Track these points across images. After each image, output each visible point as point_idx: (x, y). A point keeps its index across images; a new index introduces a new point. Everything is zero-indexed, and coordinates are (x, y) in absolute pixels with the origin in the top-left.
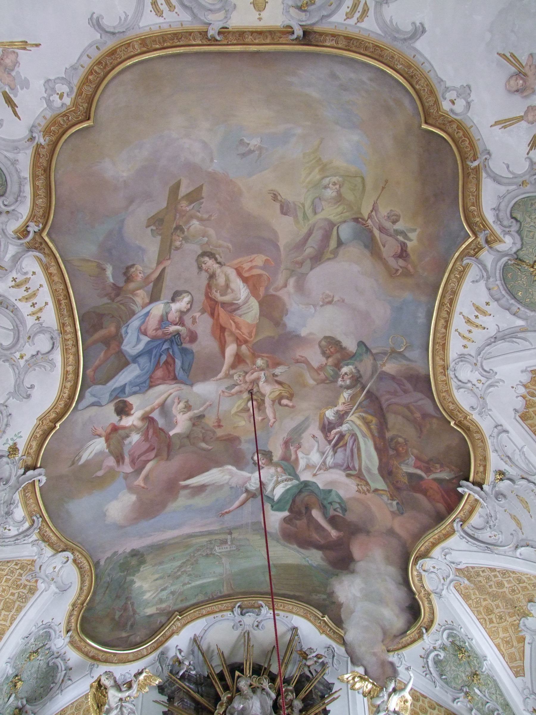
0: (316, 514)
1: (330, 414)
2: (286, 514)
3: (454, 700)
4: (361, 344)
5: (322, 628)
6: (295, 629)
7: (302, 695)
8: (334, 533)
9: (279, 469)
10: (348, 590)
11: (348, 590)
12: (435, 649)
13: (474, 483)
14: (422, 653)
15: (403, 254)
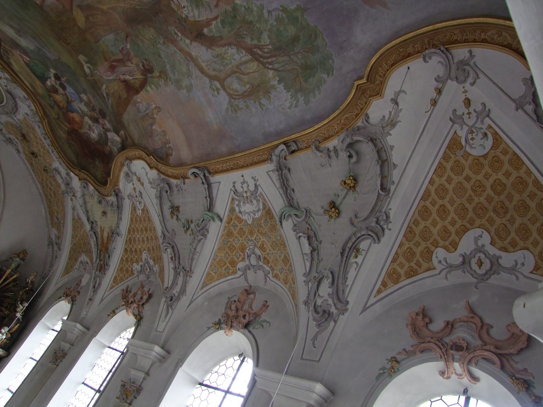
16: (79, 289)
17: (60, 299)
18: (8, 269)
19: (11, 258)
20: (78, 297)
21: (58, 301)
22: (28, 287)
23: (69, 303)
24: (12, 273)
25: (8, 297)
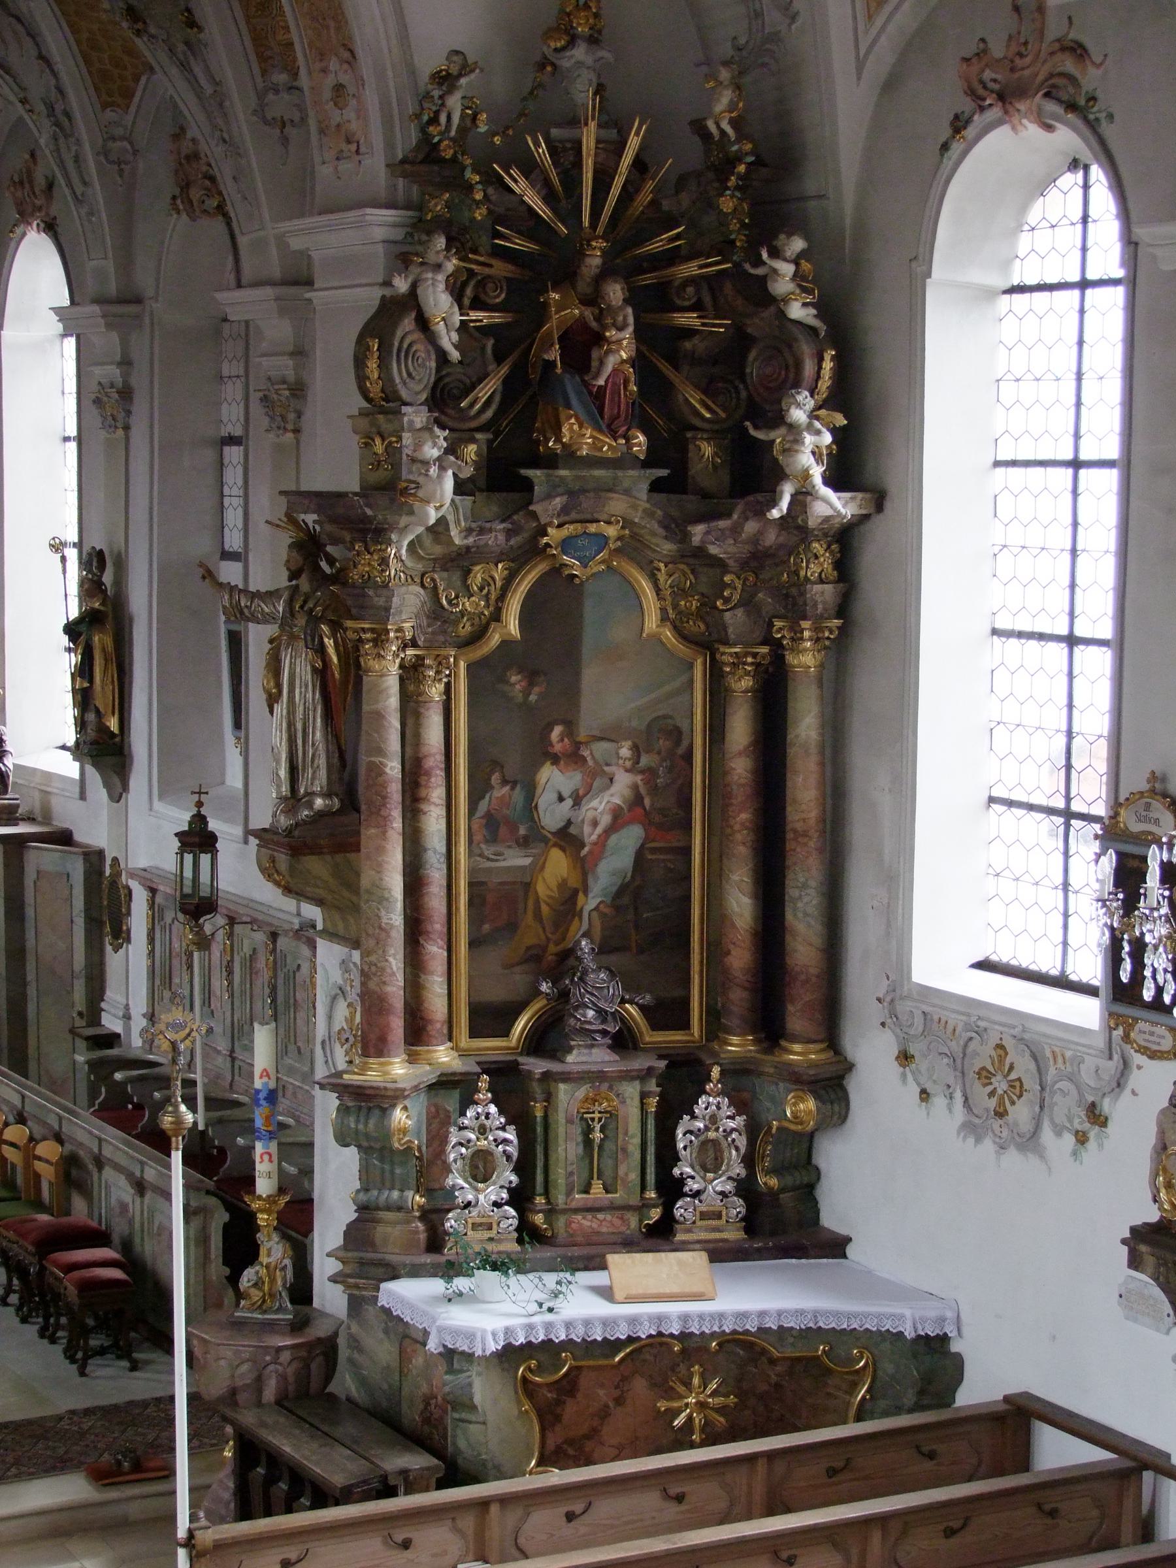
16: (1055, 29)
17: (970, 132)
18: (575, 122)
19: (541, 66)
20: (1090, 78)
21: (957, 147)
22: (738, 159)
23: (1049, 128)
24: (603, 132)
25: (672, 257)
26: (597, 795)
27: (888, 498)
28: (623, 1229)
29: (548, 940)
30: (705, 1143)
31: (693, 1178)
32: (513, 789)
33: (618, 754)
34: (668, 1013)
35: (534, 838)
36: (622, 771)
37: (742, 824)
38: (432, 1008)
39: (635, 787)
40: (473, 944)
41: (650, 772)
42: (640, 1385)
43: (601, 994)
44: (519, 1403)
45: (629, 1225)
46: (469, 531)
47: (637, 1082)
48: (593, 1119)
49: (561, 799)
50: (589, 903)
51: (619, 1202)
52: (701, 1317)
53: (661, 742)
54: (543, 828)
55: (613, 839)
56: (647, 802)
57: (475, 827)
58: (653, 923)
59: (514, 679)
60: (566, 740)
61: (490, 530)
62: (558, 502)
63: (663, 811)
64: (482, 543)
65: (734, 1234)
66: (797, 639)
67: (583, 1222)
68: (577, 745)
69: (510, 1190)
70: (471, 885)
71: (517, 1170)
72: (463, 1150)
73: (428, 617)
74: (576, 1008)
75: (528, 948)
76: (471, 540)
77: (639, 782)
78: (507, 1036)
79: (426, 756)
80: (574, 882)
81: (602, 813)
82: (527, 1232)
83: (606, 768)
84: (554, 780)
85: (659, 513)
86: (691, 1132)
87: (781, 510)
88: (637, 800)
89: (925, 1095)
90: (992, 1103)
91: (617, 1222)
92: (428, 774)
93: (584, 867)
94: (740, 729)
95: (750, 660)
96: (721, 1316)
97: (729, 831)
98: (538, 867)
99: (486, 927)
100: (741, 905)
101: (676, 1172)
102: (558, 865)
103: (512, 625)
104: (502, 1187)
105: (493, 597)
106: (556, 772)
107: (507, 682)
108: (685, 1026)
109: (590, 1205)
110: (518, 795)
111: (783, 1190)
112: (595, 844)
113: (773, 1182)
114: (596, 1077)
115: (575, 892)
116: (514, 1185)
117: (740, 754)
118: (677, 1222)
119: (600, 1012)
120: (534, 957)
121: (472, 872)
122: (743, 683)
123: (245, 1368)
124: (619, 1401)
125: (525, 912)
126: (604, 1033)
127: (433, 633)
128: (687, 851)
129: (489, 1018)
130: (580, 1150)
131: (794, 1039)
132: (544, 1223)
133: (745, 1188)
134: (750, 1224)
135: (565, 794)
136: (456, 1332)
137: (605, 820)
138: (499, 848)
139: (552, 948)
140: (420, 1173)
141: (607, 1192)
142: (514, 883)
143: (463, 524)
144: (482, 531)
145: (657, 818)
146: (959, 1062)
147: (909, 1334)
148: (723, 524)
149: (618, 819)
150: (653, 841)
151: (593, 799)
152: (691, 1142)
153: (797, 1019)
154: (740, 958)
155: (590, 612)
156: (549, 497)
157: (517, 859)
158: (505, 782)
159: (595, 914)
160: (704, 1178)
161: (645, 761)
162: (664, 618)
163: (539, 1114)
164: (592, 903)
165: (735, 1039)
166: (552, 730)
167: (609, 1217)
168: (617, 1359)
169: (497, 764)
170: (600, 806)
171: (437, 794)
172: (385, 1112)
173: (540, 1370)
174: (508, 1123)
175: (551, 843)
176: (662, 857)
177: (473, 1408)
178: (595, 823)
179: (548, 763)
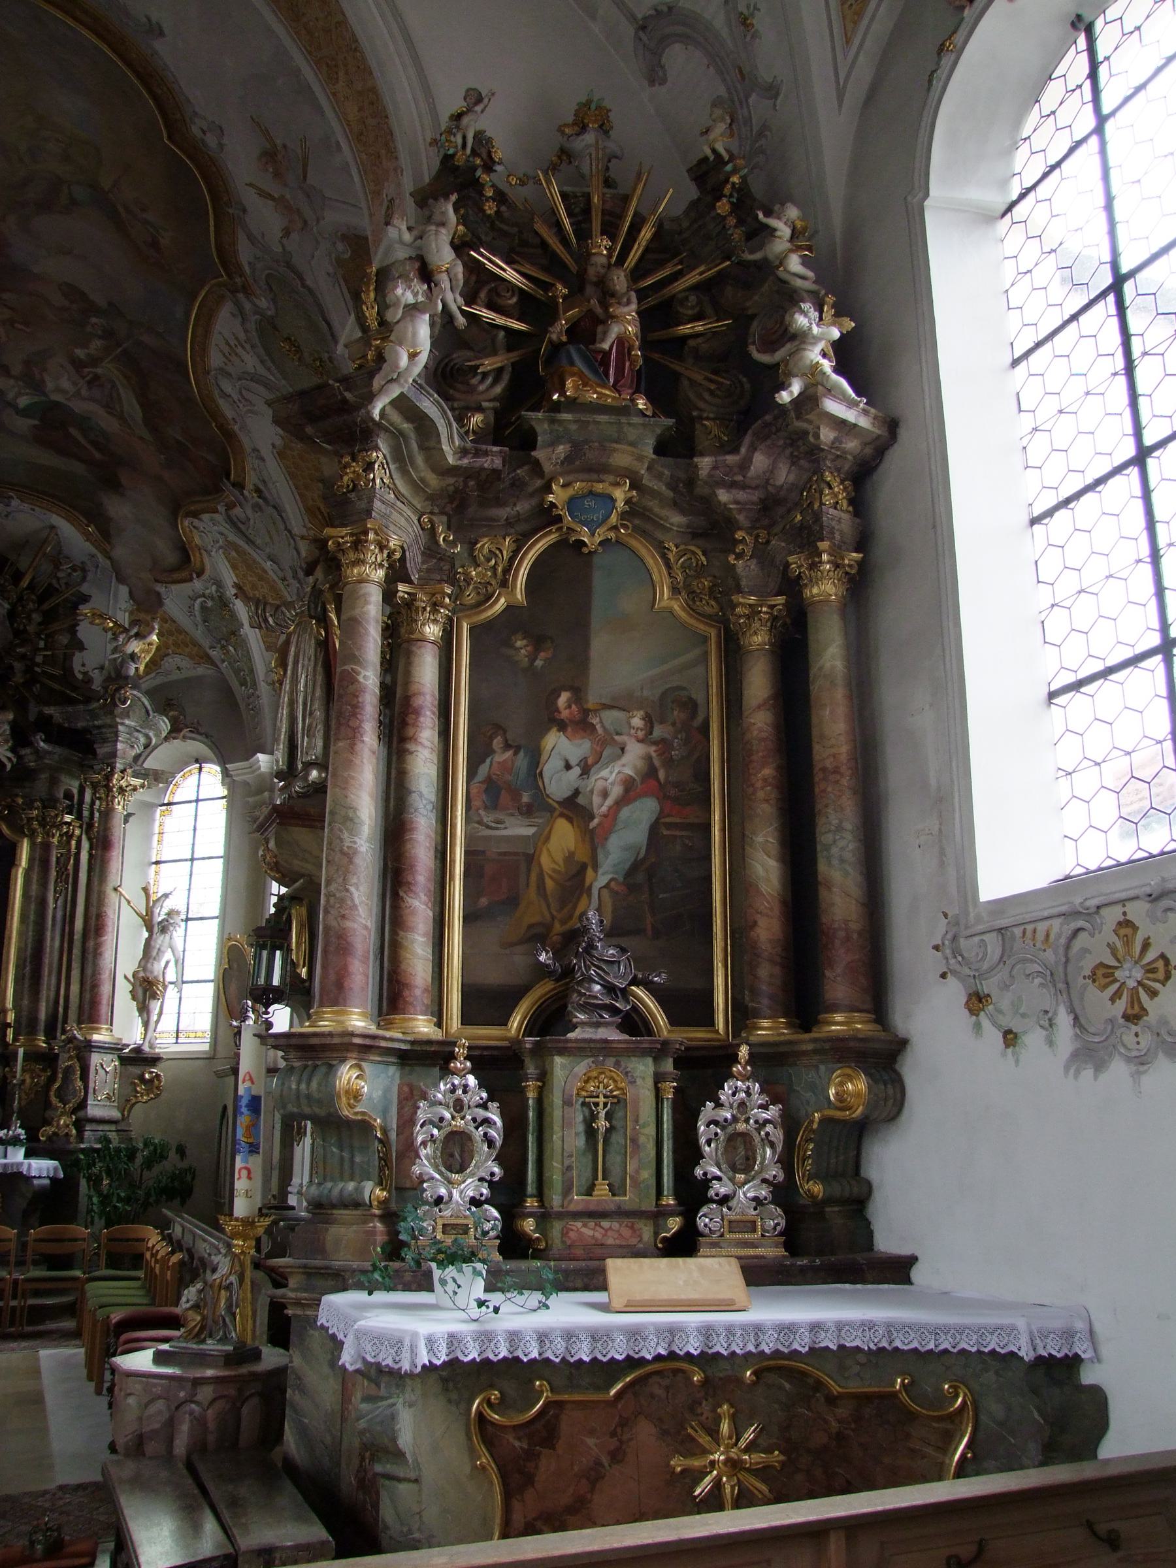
0: (73, 431)
1: (80, 353)
2: (36, 422)
3: (211, 648)
4: (110, 304)
5: (88, 536)
6: (53, 527)
7: (45, 607)
8: (97, 455)
9: (21, 383)
10: (118, 509)
11: (118, 509)
12: (204, 595)
13: (234, 485)
14: (191, 594)
15: (154, 244)
26: (606, 765)
27: (901, 424)
28: (634, 1241)
29: (553, 918)
30: (732, 1138)
31: (719, 1179)
32: (516, 754)
33: (629, 724)
34: (689, 1006)
35: (538, 806)
36: (633, 740)
37: (765, 780)
38: (410, 970)
39: (648, 758)
40: (467, 919)
41: (664, 745)
42: (645, 1432)
43: (609, 965)
44: (473, 1454)
45: (640, 1236)
46: (463, 452)
47: (650, 1060)
48: (596, 1105)
49: (568, 767)
50: (600, 879)
51: (627, 1207)
52: (730, 1330)
53: (676, 713)
54: (548, 796)
55: (625, 812)
56: (662, 774)
57: (474, 791)
58: (668, 903)
59: (519, 644)
60: (574, 706)
61: (486, 453)
62: (562, 450)
63: (679, 785)
64: (477, 465)
65: (772, 1251)
66: (814, 566)
67: (584, 1230)
68: (586, 712)
69: (491, 1185)
70: (468, 853)
71: (499, 1159)
72: (435, 1132)
73: (423, 554)
74: (580, 983)
75: (531, 926)
76: (465, 461)
77: (654, 755)
78: (506, 1025)
79: (414, 695)
80: (582, 856)
81: (612, 784)
82: (513, 1244)
83: (616, 737)
84: (560, 747)
85: (666, 472)
86: (716, 1123)
87: (791, 392)
88: (650, 772)
89: (1010, 1038)
90: (1121, 1005)
91: (626, 1232)
92: (417, 712)
93: (594, 839)
94: (758, 683)
95: (764, 609)
96: (758, 1328)
97: (750, 790)
98: (543, 837)
99: (484, 901)
100: (767, 870)
101: (699, 1172)
102: (564, 837)
103: (520, 595)
104: (481, 1179)
105: (500, 569)
106: (563, 738)
107: (512, 647)
108: (708, 1020)
109: (592, 1207)
110: (522, 761)
111: (828, 1200)
112: (605, 816)
113: (817, 1188)
114: (603, 1049)
115: (583, 868)
116: (496, 1179)
117: (759, 707)
118: (702, 1235)
119: (610, 989)
120: (537, 937)
121: (469, 839)
122: (759, 639)
123: (160, 1405)
124: (616, 1456)
125: (528, 885)
126: (614, 1011)
127: (428, 571)
128: (707, 828)
129: (484, 1003)
130: (581, 1142)
131: (834, 1008)
132: (535, 1231)
133: (783, 1194)
134: (791, 1239)
135: (573, 762)
136: (379, 1338)
137: (616, 791)
138: (500, 816)
139: (558, 928)
140: (385, 1160)
141: (614, 1195)
142: (515, 854)
143: (457, 444)
144: (478, 453)
145: (673, 792)
146: (1060, 981)
147: (1027, 1354)
148: (731, 459)
149: (630, 791)
150: (668, 816)
151: (604, 768)
152: (716, 1134)
153: (838, 984)
154: (768, 929)
155: (599, 582)
156: (553, 444)
157: (519, 829)
158: (507, 746)
159: (605, 892)
160: (732, 1180)
161: (658, 732)
162: (675, 590)
163: (531, 1095)
164: (602, 880)
165: (765, 1023)
166: (559, 696)
167: (615, 1225)
168: (613, 1392)
169: (499, 728)
170: (610, 777)
171: (427, 733)
172: (331, 1069)
173: (501, 1406)
174: (491, 1098)
175: (557, 813)
176: (678, 833)
177: (399, 1455)
178: (605, 794)
179: (555, 729)
